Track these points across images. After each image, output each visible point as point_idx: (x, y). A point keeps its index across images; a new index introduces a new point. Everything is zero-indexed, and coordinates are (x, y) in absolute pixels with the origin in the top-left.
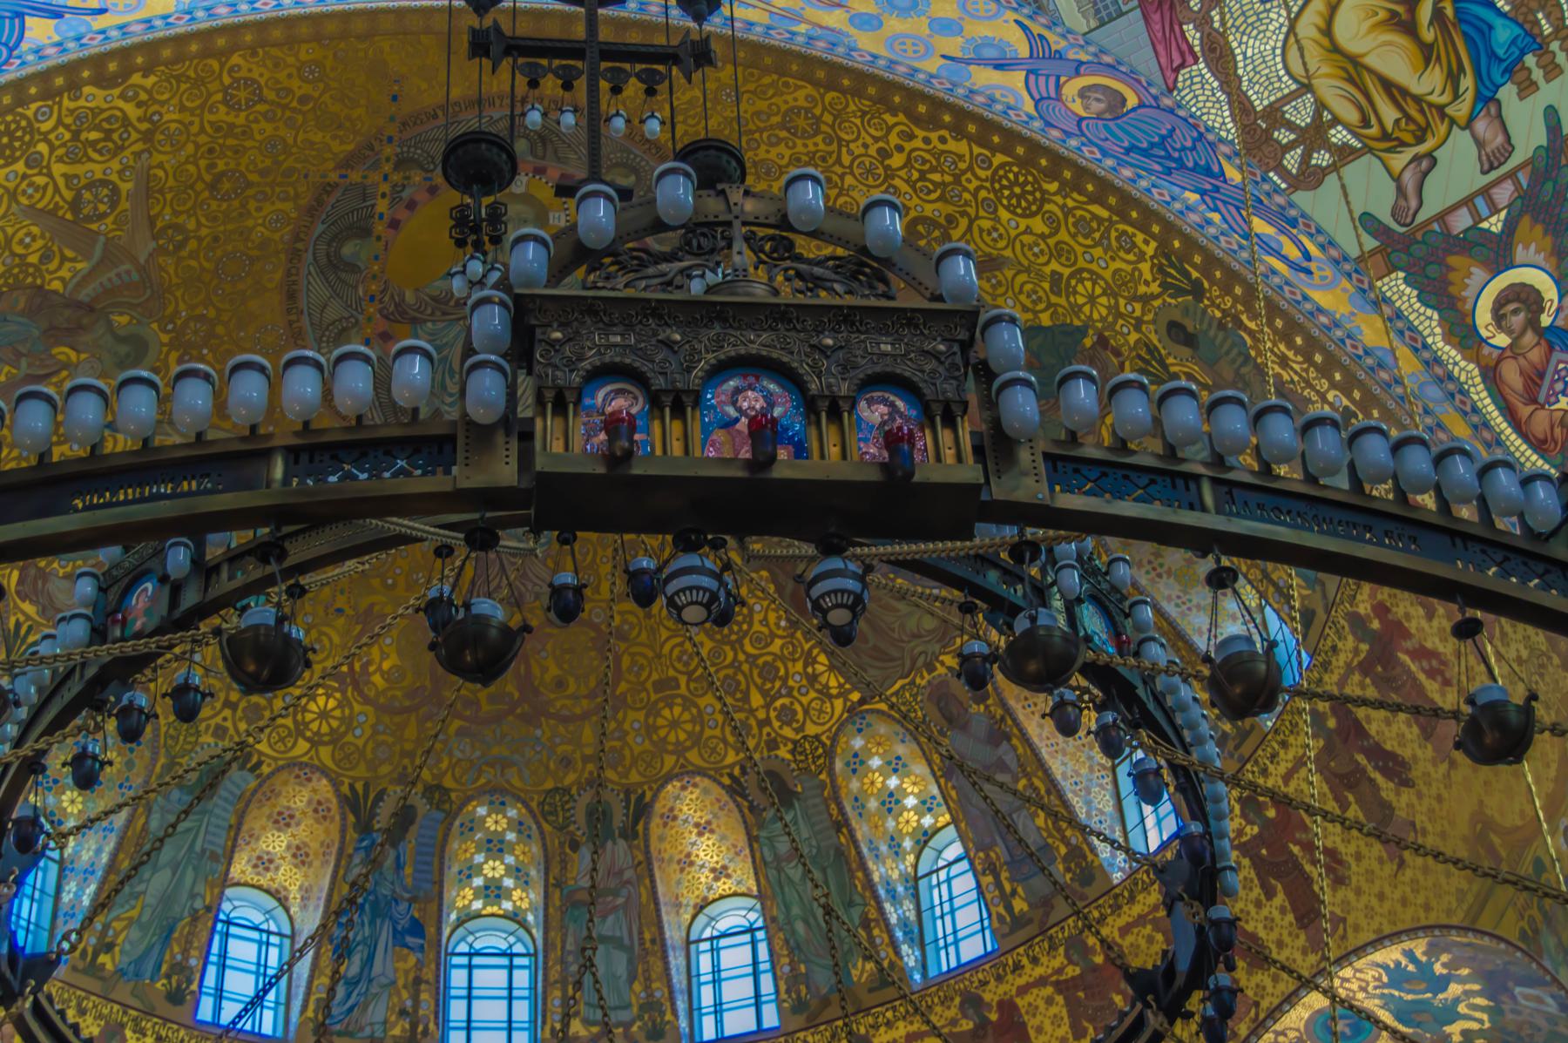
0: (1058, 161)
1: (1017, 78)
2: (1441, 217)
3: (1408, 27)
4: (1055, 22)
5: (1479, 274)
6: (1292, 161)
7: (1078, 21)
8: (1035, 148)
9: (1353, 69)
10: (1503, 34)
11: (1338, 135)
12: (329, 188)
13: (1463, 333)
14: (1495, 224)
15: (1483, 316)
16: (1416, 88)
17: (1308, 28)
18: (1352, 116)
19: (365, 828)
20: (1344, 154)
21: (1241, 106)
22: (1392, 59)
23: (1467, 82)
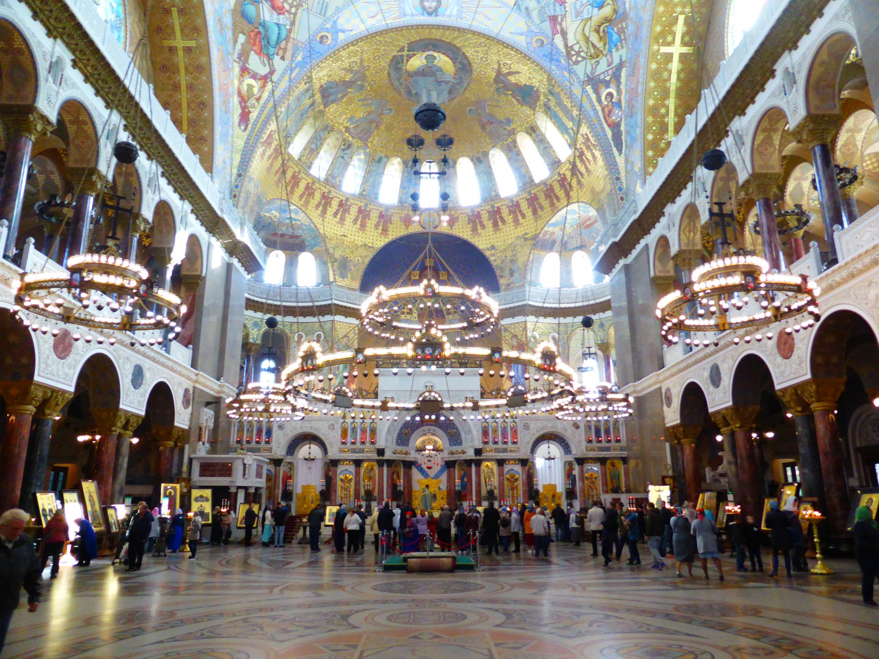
0: (529, 59)
1: (523, 38)
2: (599, 75)
3: (598, 32)
4: (533, 22)
5: (603, 88)
6: (574, 58)
7: (537, 21)
8: (526, 56)
9: (587, 40)
10: (615, 37)
11: (583, 54)
12: (394, 56)
13: (599, 100)
14: (608, 78)
15: (603, 98)
16: (598, 46)
17: (580, 30)
18: (585, 49)
19: (407, 167)
20: (584, 58)
21: (566, 45)
22: (594, 38)
23: (607, 46)
